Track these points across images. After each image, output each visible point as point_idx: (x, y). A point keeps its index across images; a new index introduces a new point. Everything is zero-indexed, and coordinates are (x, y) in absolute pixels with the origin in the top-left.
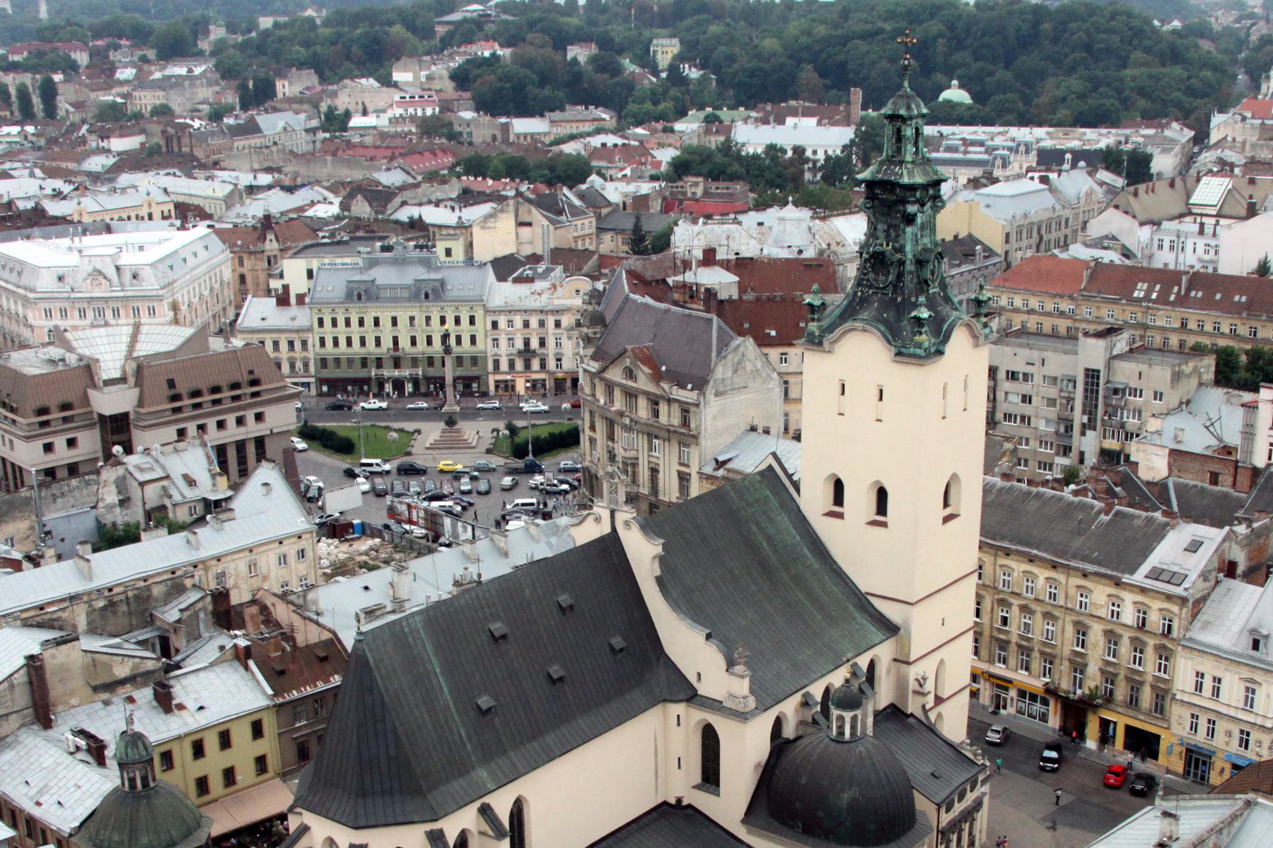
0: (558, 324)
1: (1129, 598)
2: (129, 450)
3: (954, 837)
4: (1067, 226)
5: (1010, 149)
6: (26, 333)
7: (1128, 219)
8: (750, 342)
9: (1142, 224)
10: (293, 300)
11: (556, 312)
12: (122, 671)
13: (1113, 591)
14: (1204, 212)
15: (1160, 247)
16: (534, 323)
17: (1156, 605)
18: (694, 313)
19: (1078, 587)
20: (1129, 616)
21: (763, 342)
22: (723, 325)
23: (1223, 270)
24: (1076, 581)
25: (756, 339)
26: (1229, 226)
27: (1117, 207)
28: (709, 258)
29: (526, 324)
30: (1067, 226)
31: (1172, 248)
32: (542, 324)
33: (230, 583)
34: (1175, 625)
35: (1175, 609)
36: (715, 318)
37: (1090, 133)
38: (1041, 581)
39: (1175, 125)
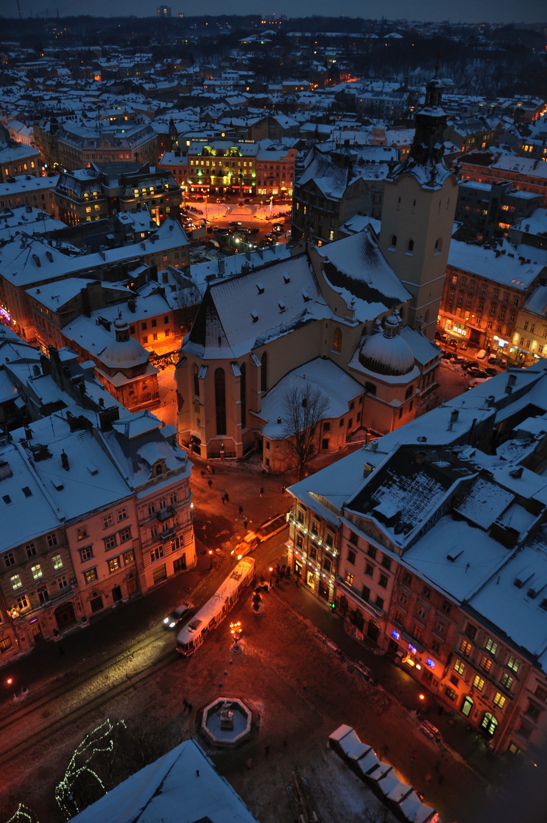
0: (284, 168)
1: (502, 290)
2: (119, 211)
3: (427, 377)
5: (468, 104)
6: (79, 164)
10: (181, 154)
11: (284, 163)
12: (117, 296)
13: (497, 287)
16: (275, 167)
17: (513, 294)
19: (483, 285)
20: (501, 297)
24: (481, 282)
29: (272, 168)
32: (278, 168)
33: (157, 264)
34: (519, 302)
35: (520, 296)
37: (501, 100)
38: (468, 281)
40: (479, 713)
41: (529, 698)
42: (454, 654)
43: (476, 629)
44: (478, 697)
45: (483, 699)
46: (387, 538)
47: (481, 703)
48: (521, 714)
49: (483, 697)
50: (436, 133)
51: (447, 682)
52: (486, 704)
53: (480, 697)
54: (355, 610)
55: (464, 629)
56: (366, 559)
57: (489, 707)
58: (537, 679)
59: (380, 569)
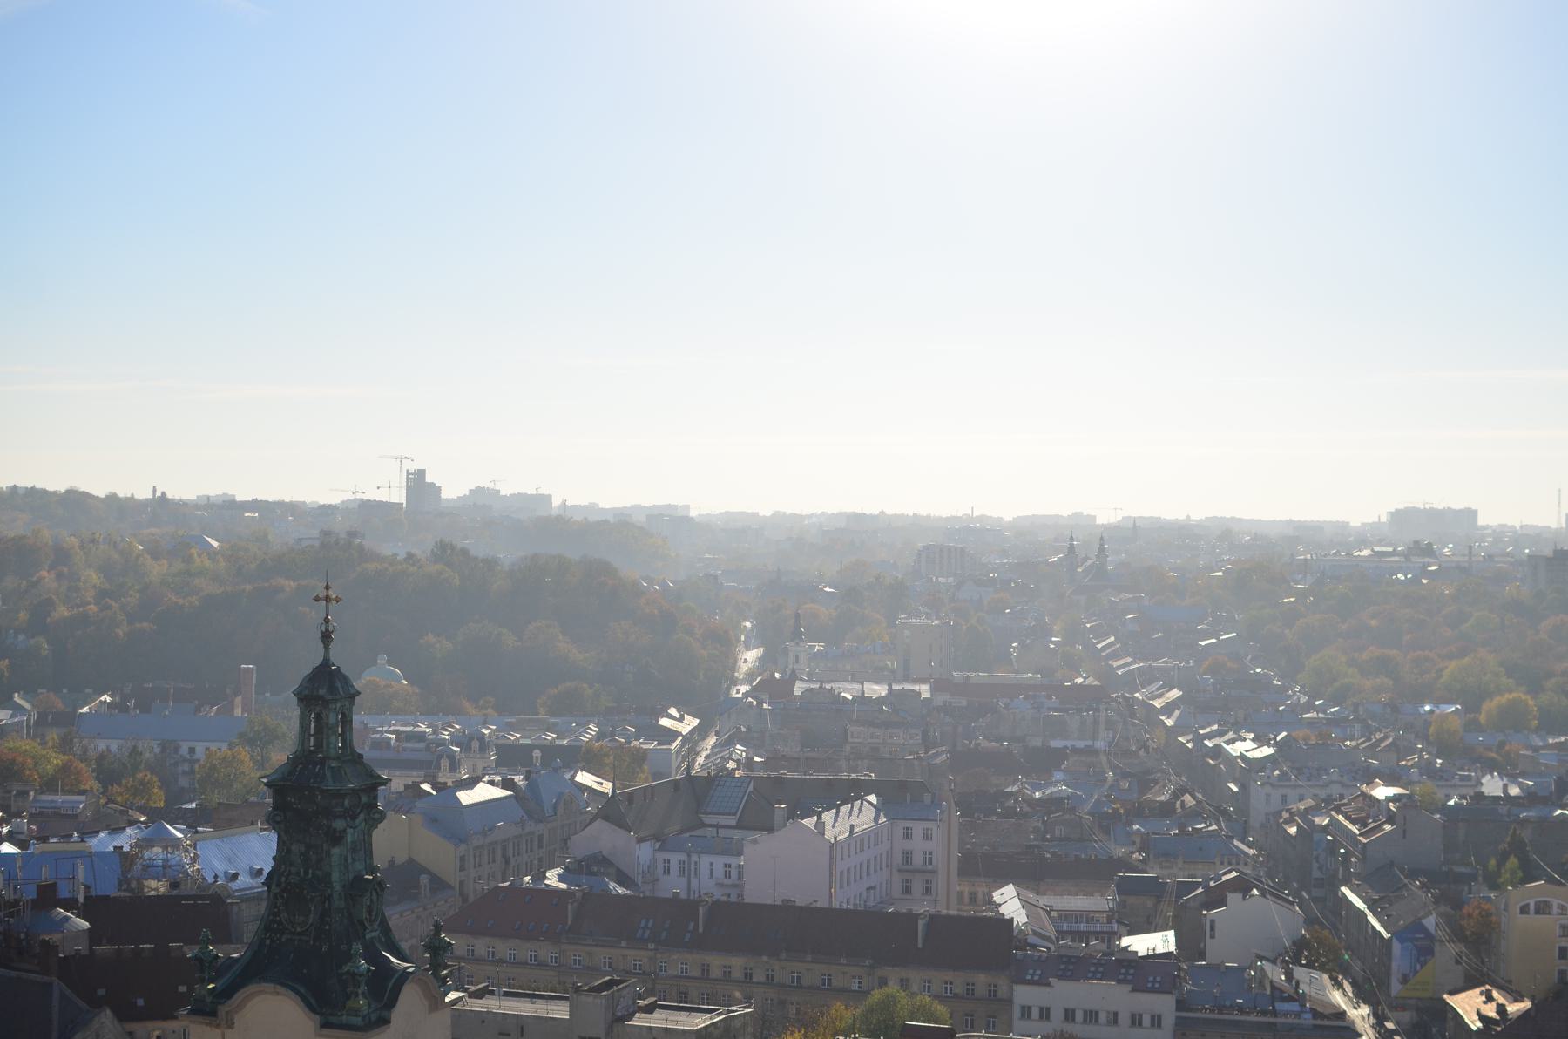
4: (540, 847)
7: (622, 832)
8: (106, 1017)
9: (640, 841)
14: (722, 822)
15: (667, 871)
18: (25, 975)
21: (126, 1014)
22: (68, 992)
23: (747, 900)
25: (113, 1010)
26: (755, 841)
27: (606, 818)
28: (48, 896)
30: (540, 847)
31: (681, 872)
36: (56, 981)
39: (673, 711)
50: (349, 839)
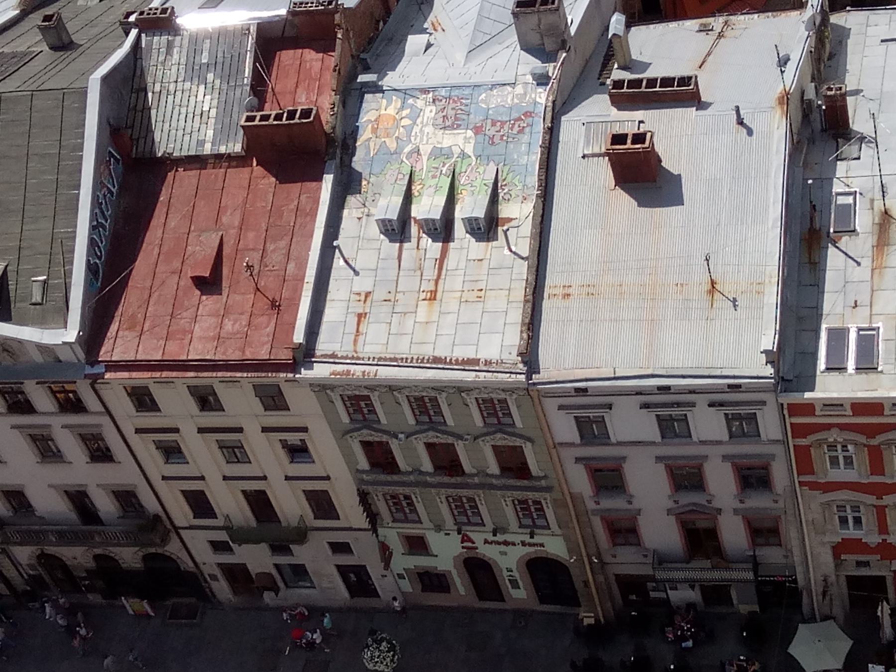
40: (516, 574)
41: (578, 460)
42: (370, 489)
43: (368, 398)
44: (486, 542)
45: (500, 538)
46: (20, 342)
47: (503, 548)
48: (591, 505)
49: (495, 535)
51: (402, 562)
52: (514, 544)
53: (491, 538)
54: (91, 564)
55: (346, 419)
56: (13, 427)
57: (524, 544)
58: (561, 407)
59: (64, 427)
